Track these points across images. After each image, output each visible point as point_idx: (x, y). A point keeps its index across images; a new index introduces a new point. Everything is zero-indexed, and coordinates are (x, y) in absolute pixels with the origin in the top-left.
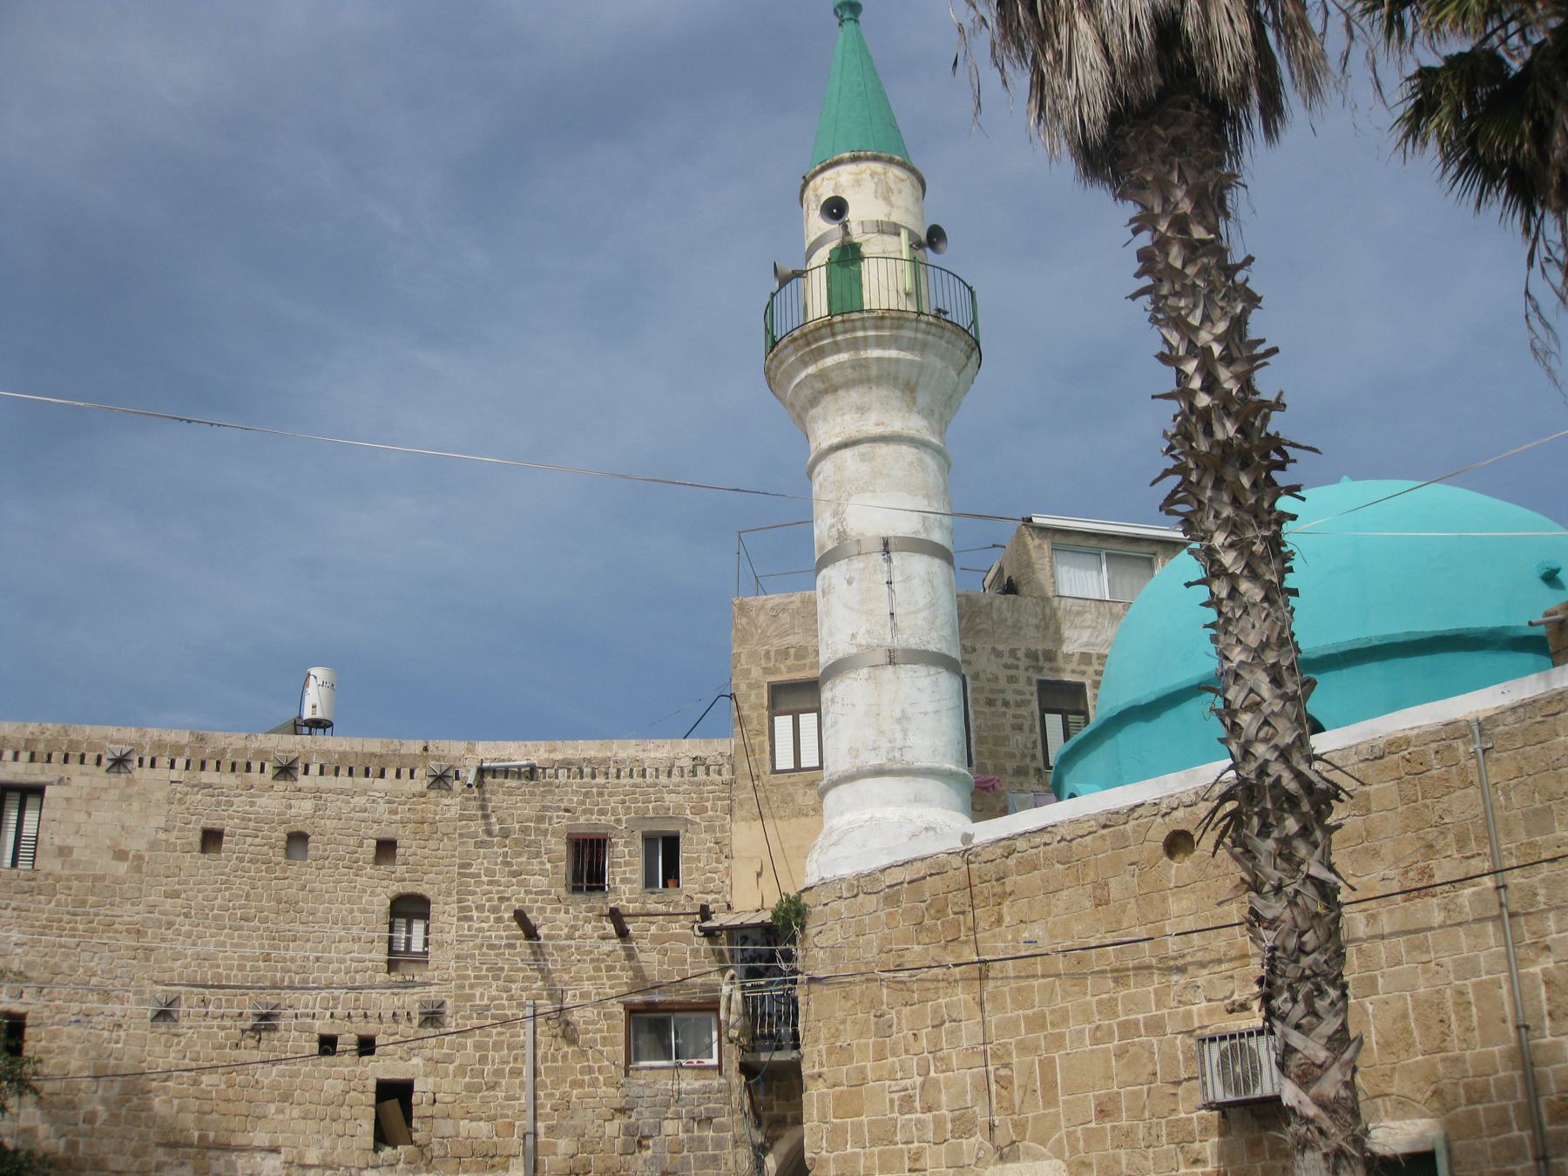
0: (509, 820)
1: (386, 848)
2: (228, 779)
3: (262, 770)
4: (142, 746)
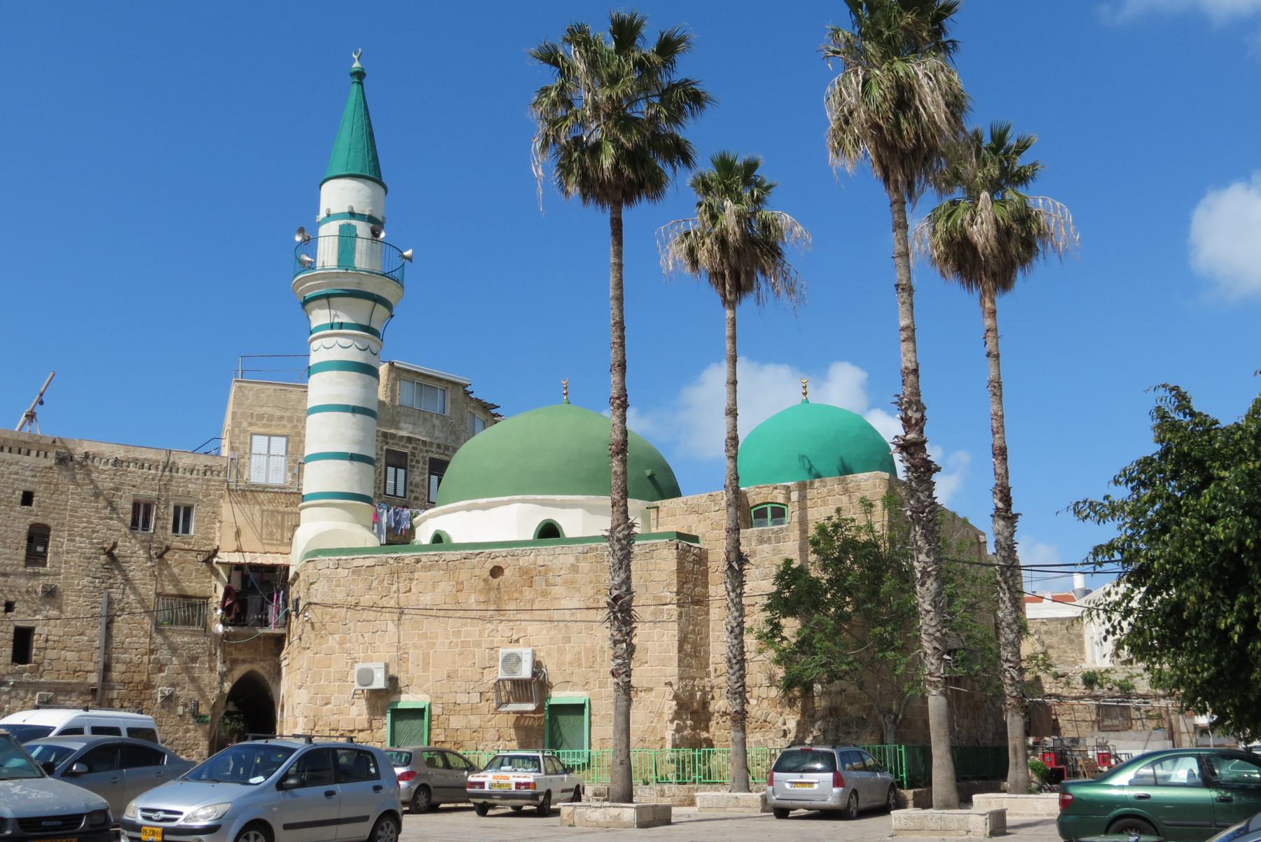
1: (27, 498)
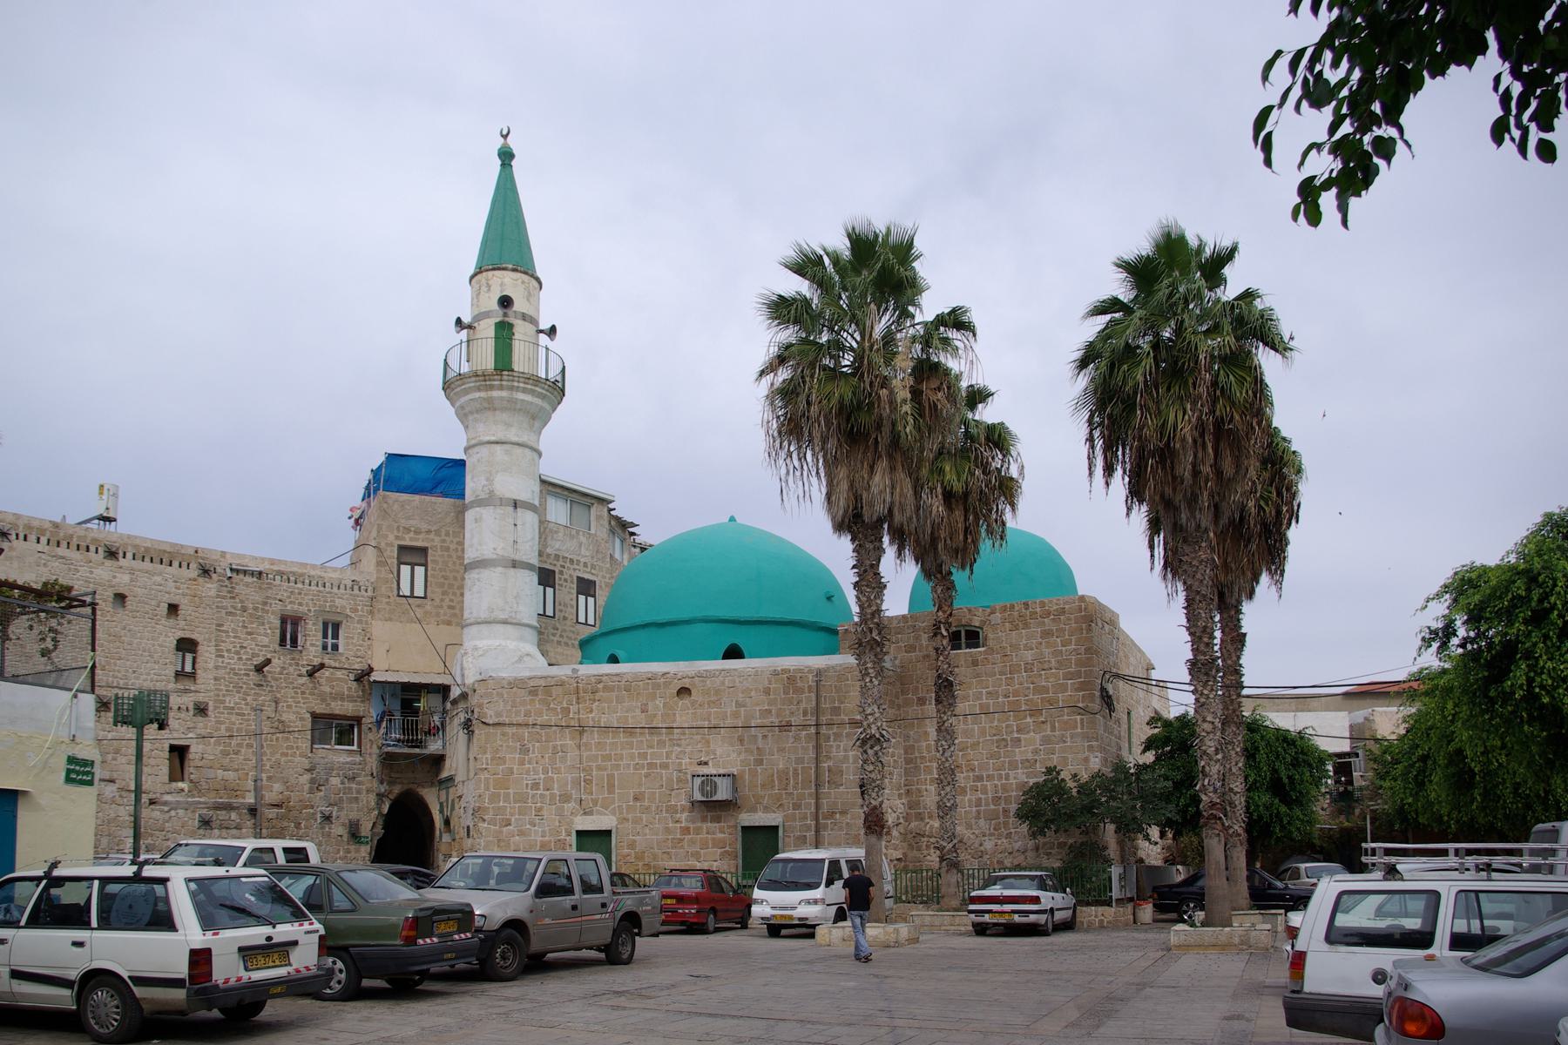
1: (173, 609)
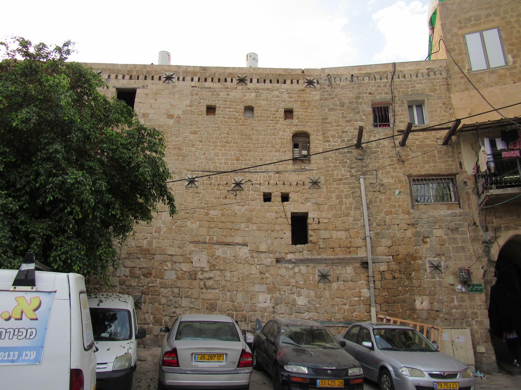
0: (344, 99)
1: (289, 113)
2: (217, 85)
3: (232, 81)
4: (179, 73)
